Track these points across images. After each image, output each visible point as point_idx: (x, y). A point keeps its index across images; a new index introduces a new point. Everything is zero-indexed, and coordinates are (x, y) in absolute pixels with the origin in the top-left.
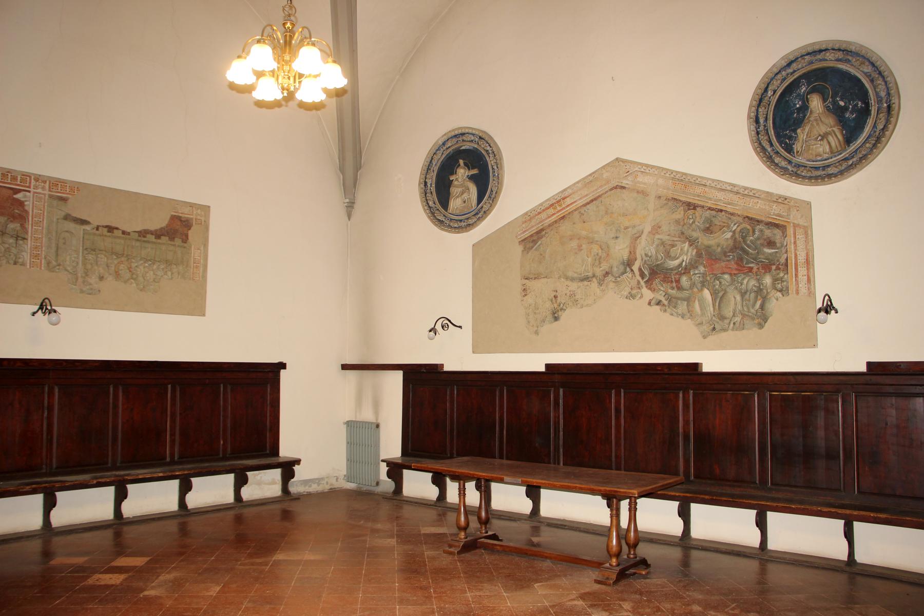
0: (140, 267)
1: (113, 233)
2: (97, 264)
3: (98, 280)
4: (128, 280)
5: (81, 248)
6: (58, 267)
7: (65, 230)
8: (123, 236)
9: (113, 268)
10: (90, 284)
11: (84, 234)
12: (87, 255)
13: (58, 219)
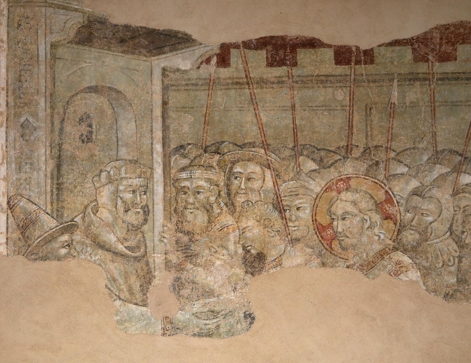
0: (435, 192)
1: (295, 64)
2: (231, 205)
3: (239, 271)
4: (382, 254)
5: (158, 147)
6: (65, 237)
7: (86, 85)
8: (342, 70)
9: (306, 214)
10: (209, 293)
11: (165, 89)
12: (184, 175)
13: (54, 46)
